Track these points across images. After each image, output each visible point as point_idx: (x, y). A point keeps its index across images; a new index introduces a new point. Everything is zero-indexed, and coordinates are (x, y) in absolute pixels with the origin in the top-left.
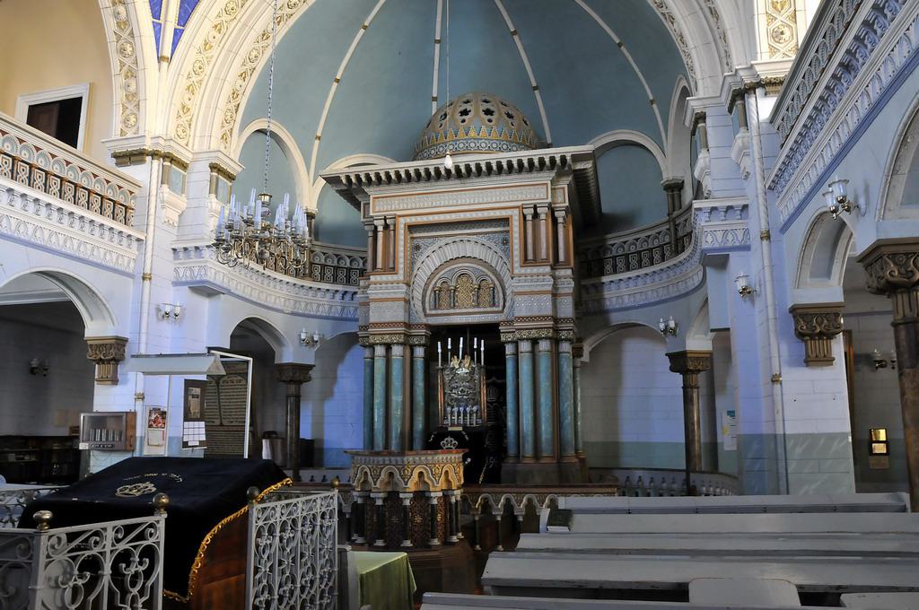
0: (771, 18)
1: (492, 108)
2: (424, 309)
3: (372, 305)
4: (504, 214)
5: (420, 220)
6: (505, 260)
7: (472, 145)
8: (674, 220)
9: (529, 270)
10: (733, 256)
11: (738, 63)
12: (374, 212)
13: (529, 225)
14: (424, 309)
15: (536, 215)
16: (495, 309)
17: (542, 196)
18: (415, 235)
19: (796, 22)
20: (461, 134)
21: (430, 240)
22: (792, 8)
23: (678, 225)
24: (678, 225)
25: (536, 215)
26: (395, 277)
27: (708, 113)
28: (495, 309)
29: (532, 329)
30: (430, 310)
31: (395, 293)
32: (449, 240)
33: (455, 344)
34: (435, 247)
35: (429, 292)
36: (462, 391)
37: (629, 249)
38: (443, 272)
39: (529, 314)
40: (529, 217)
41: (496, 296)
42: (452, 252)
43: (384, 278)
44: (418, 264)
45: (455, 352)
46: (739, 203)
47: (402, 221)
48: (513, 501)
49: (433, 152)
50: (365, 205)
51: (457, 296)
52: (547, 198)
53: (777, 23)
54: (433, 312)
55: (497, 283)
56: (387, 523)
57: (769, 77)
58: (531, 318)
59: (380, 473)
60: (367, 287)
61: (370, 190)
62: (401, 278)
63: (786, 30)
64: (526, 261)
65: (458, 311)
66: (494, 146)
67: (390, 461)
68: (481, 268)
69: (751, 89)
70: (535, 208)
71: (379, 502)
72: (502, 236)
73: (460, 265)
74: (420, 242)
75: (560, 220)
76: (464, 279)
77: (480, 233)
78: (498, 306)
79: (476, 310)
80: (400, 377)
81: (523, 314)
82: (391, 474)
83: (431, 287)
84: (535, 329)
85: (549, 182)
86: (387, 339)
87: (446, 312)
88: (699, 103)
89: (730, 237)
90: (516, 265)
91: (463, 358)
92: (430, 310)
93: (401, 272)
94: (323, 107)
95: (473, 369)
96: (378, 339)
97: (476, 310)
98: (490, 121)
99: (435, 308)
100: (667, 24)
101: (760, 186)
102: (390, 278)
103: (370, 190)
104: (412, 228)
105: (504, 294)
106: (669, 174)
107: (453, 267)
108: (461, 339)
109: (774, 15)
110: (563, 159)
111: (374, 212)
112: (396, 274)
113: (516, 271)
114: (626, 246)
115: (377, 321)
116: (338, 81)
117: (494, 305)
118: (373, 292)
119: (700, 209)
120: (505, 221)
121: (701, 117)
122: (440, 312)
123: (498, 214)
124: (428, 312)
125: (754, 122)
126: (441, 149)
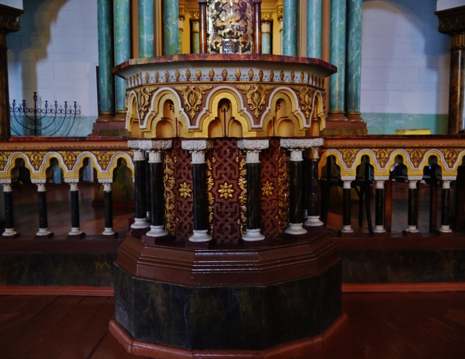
36: (230, 33)
48: (373, 161)
56: (211, 198)
80: (150, 12)
82: (225, 103)
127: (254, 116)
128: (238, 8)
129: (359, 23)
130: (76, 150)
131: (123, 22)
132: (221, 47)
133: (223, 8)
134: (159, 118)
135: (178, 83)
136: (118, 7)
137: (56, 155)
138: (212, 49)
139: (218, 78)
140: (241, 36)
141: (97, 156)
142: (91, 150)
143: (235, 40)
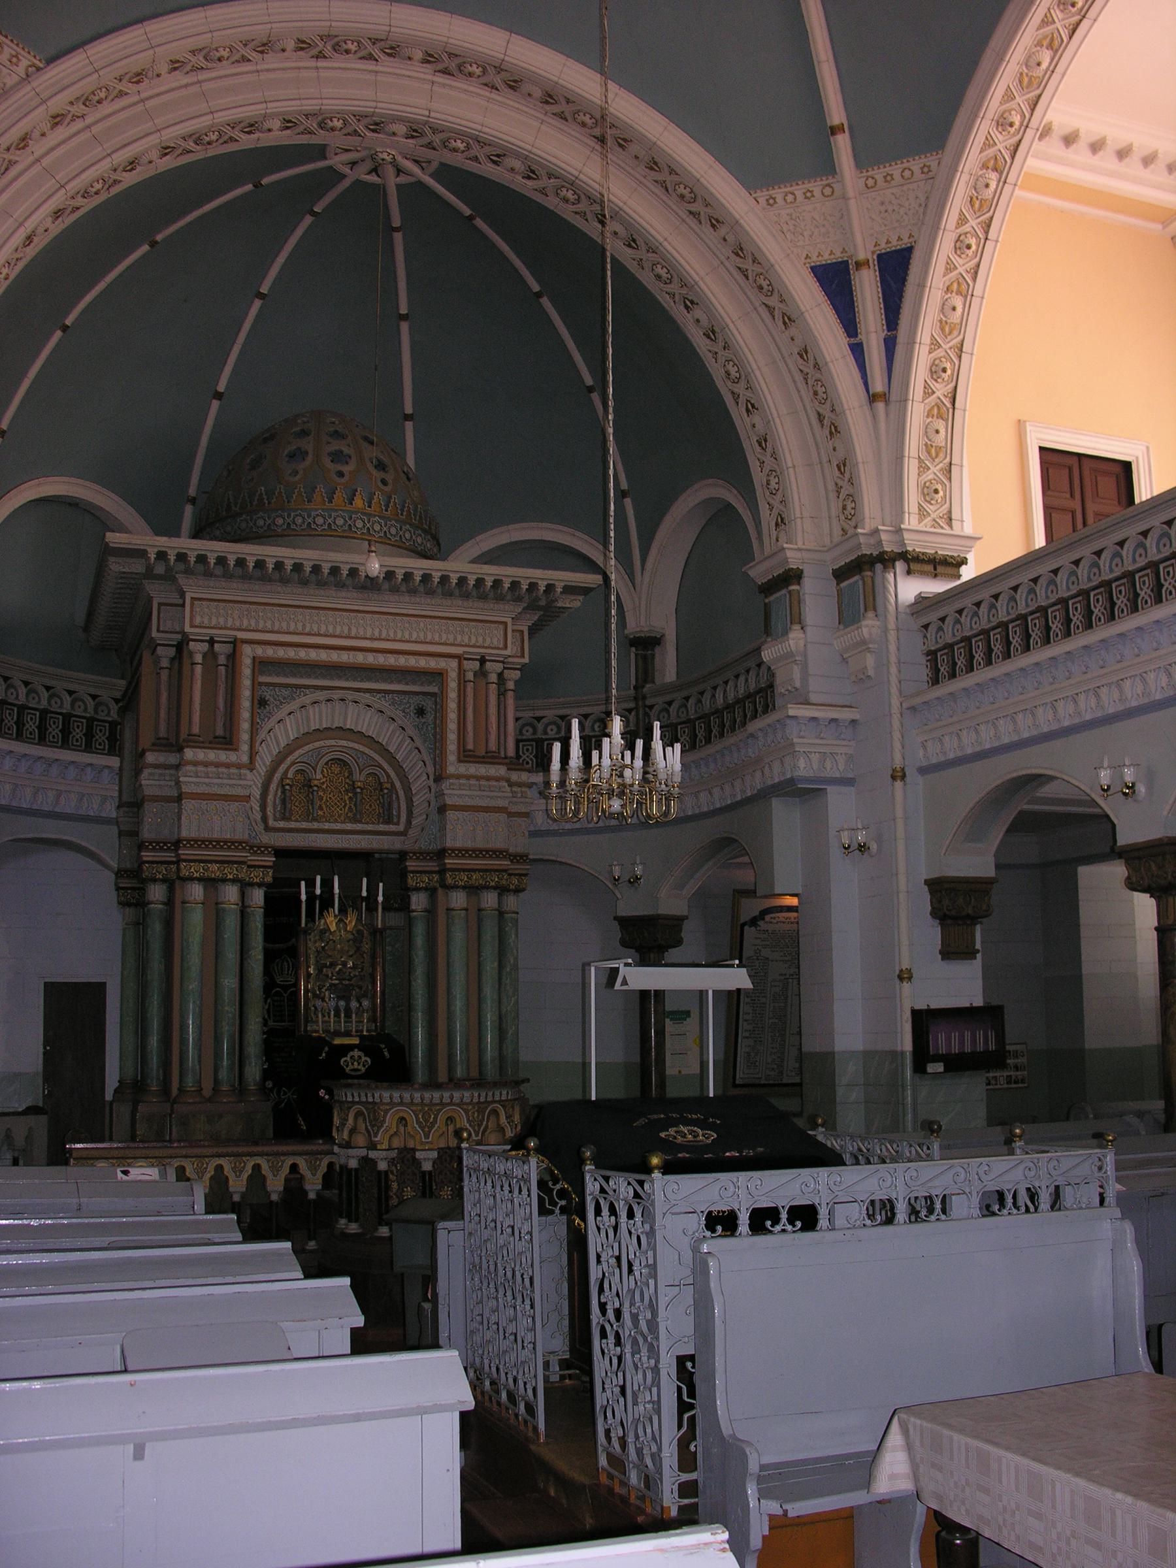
0: (923, 468)
1: (386, 460)
2: (264, 819)
3: (188, 804)
4: (432, 664)
5: (281, 653)
6: (419, 743)
7: (359, 524)
8: (644, 698)
9: (472, 769)
10: (830, 789)
11: (872, 515)
12: (192, 626)
13: (470, 686)
14: (264, 819)
15: (482, 673)
16: (393, 828)
17: (496, 643)
18: (262, 679)
19: (950, 479)
20: (339, 496)
21: (286, 692)
22: (948, 459)
23: (651, 707)
24: (651, 707)
25: (482, 673)
26: (233, 757)
27: (808, 571)
28: (393, 828)
29: (474, 870)
30: (275, 820)
31: (232, 786)
32: (320, 695)
33: (327, 884)
34: (294, 706)
35: (273, 786)
37: (545, 733)
38: (301, 751)
39: (469, 844)
40: (470, 676)
41: (395, 805)
42: (319, 718)
43: (212, 755)
44: (262, 735)
45: (327, 902)
46: (845, 715)
47: (247, 650)
49: (280, 521)
50: (160, 604)
51: (321, 799)
52: (506, 647)
53: (929, 476)
54: (282, 824)
55: (398, 785)
57: (917, 550)
58: (474, 851)
59: (385, 1117)
60: (177, 767)
61: (193, 588)
62: (245, 759)
63: (939, 487)
64: (466, 756)
65: (327, 826)
66: (393, 531)
67: (391, 1098)
68: (367, 751)
69: (886, 560)
70: (483, 661)
71: (427, 1166)
72: (415, 701)
73: (333, 742)
74: (268, 694)
75: (511, 685)
76: (336, 769)
77: (379, 691)
78: (398, 824)
79: (359, 827)
81: (458, 844)
83: (278, 776)
84: (480, 870)
85: (509, 621)
86: (215, 870)
87: (304, 825)
88: (798, 555)
89: (828, 765)
90: (452, 757)
91: (343, 910)
92: (275, 820)
93: (245, 747)
94: (25, 373)
95: (359, 932)
96: (196, 870)
97: (359, 827)
98: (384, 482)
99: (284, 818)
100: (737, 413)
101: (895, 702)
102: (223, 756)
103: (193, 588)
104: (261, 665)
105: (410, 802)
106: (636, 625)
107: (322, 743)
108: (365, 880)
109: (927, 462)
110: (550, 588)
111: (192, 626)
112: (236, 750)
113: (451, 770)
114: (540, 726)
115: (194, 835)
116: (65, 328)
117: (388, 821)
118: (190, 781)
119: (795, 717)
120: (438, 676)
121: (792, 577)
122: (293, 825)
123: (422, 663)
124: (271, 823)
125: (891, 608)
126: (299, 520)
127: (474, 1131)
128: (351, 937)
129: (516, 959)
130: (245, 1156)
131: (197, 961)
132: (327, 993)
133: (331, 937)
134: (392, 1132)
135: (412, 1104)
136: (190, 940)
137: (221, 1161)
138: (315, 996)
139: (446, 1100)
140: (355, 976)
141: (268, 1161)
142: (261, 1154)
143: (347, 982)
